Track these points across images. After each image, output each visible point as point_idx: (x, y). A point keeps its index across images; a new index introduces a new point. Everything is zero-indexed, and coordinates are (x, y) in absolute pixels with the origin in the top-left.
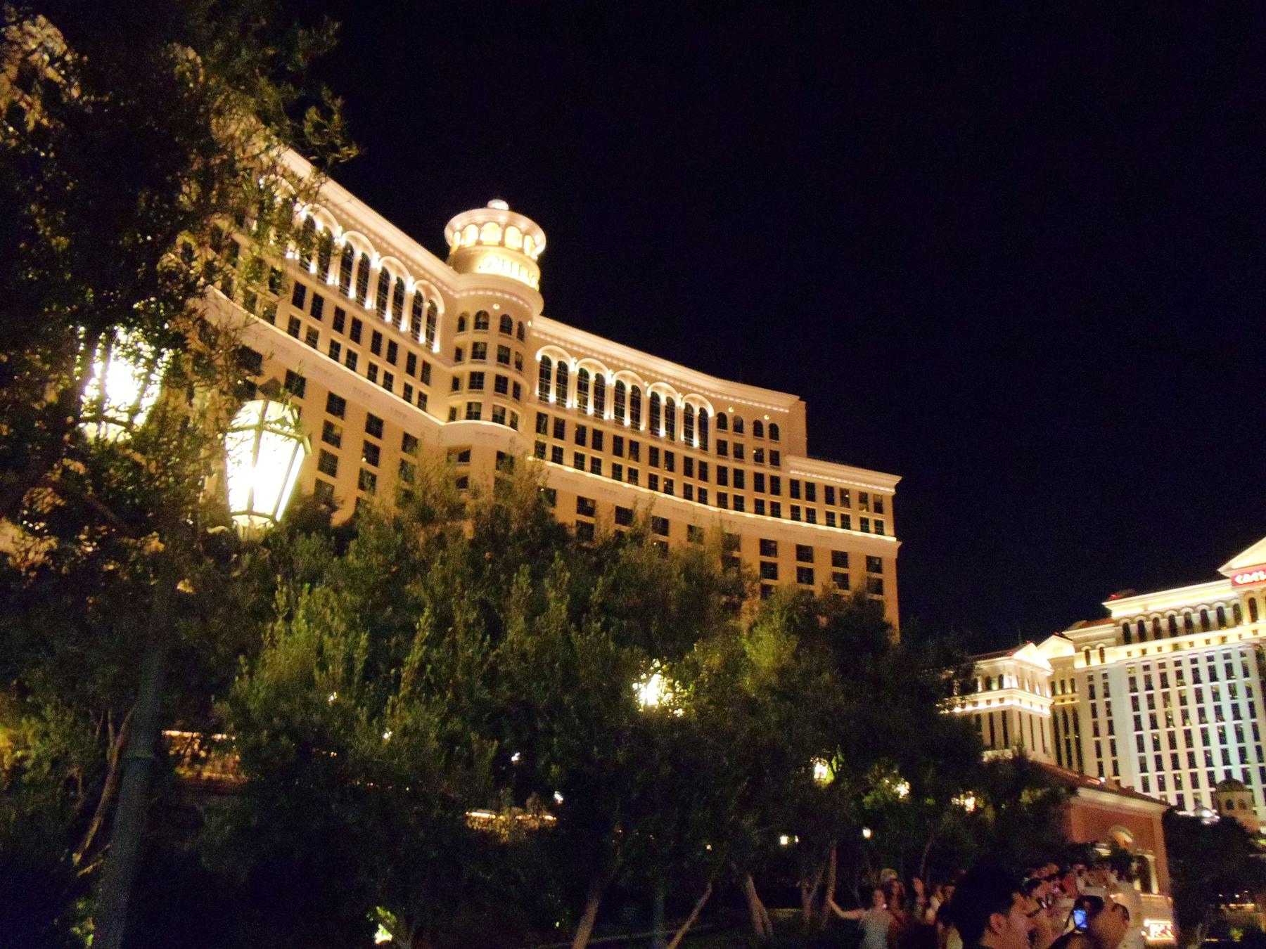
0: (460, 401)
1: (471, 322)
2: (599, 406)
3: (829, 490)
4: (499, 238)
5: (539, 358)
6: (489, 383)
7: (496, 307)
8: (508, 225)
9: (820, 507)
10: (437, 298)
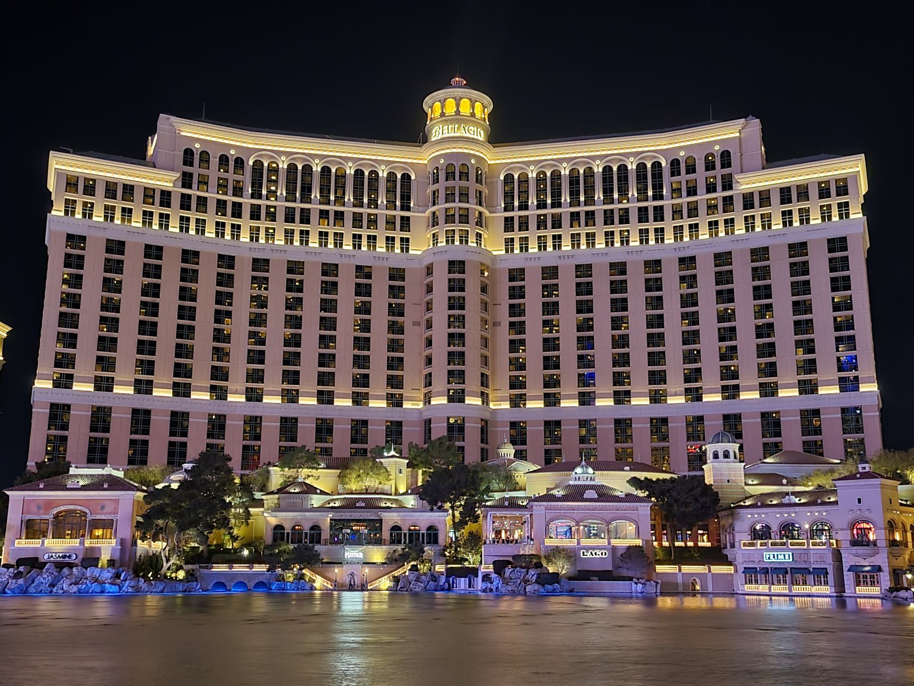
7: (442, 161)
8: (445, 99)
10: (407, 170)
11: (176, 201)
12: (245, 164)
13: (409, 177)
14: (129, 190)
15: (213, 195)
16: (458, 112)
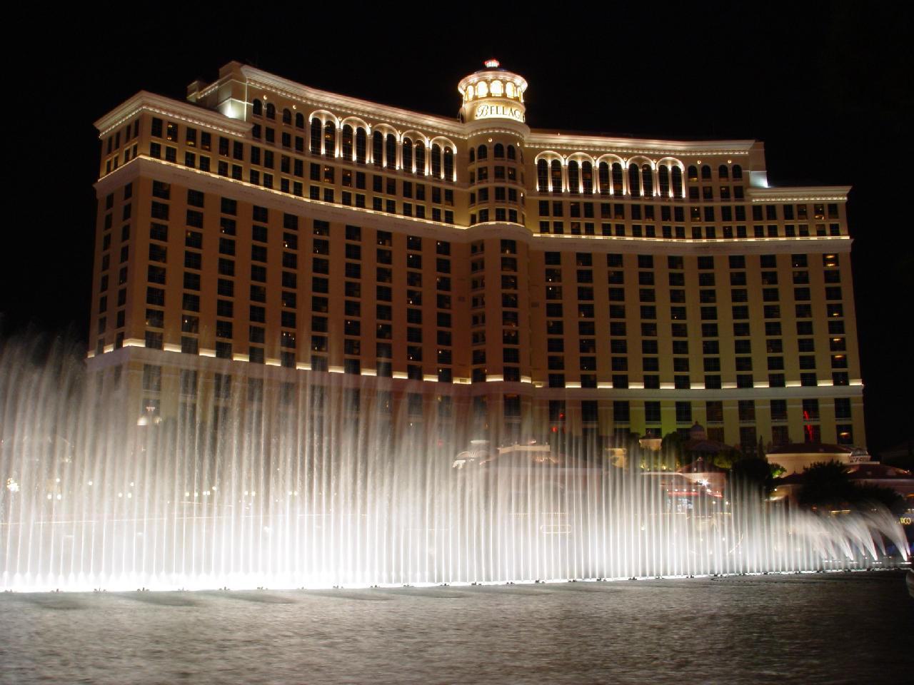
0: (475, 211)
1: (476, 153)
2: (588, 186)
3: (788, 209)
4: (487, 91)
5: (536, 163)
6: (492, 194)
7: (490, 141)
8: (492, 81)
9: (781, 223)
11: (247, 153)
12: (305, 121)
13: (451, 151)
14: (207, 137)
15: (278, 150)
16: (504, 95)
